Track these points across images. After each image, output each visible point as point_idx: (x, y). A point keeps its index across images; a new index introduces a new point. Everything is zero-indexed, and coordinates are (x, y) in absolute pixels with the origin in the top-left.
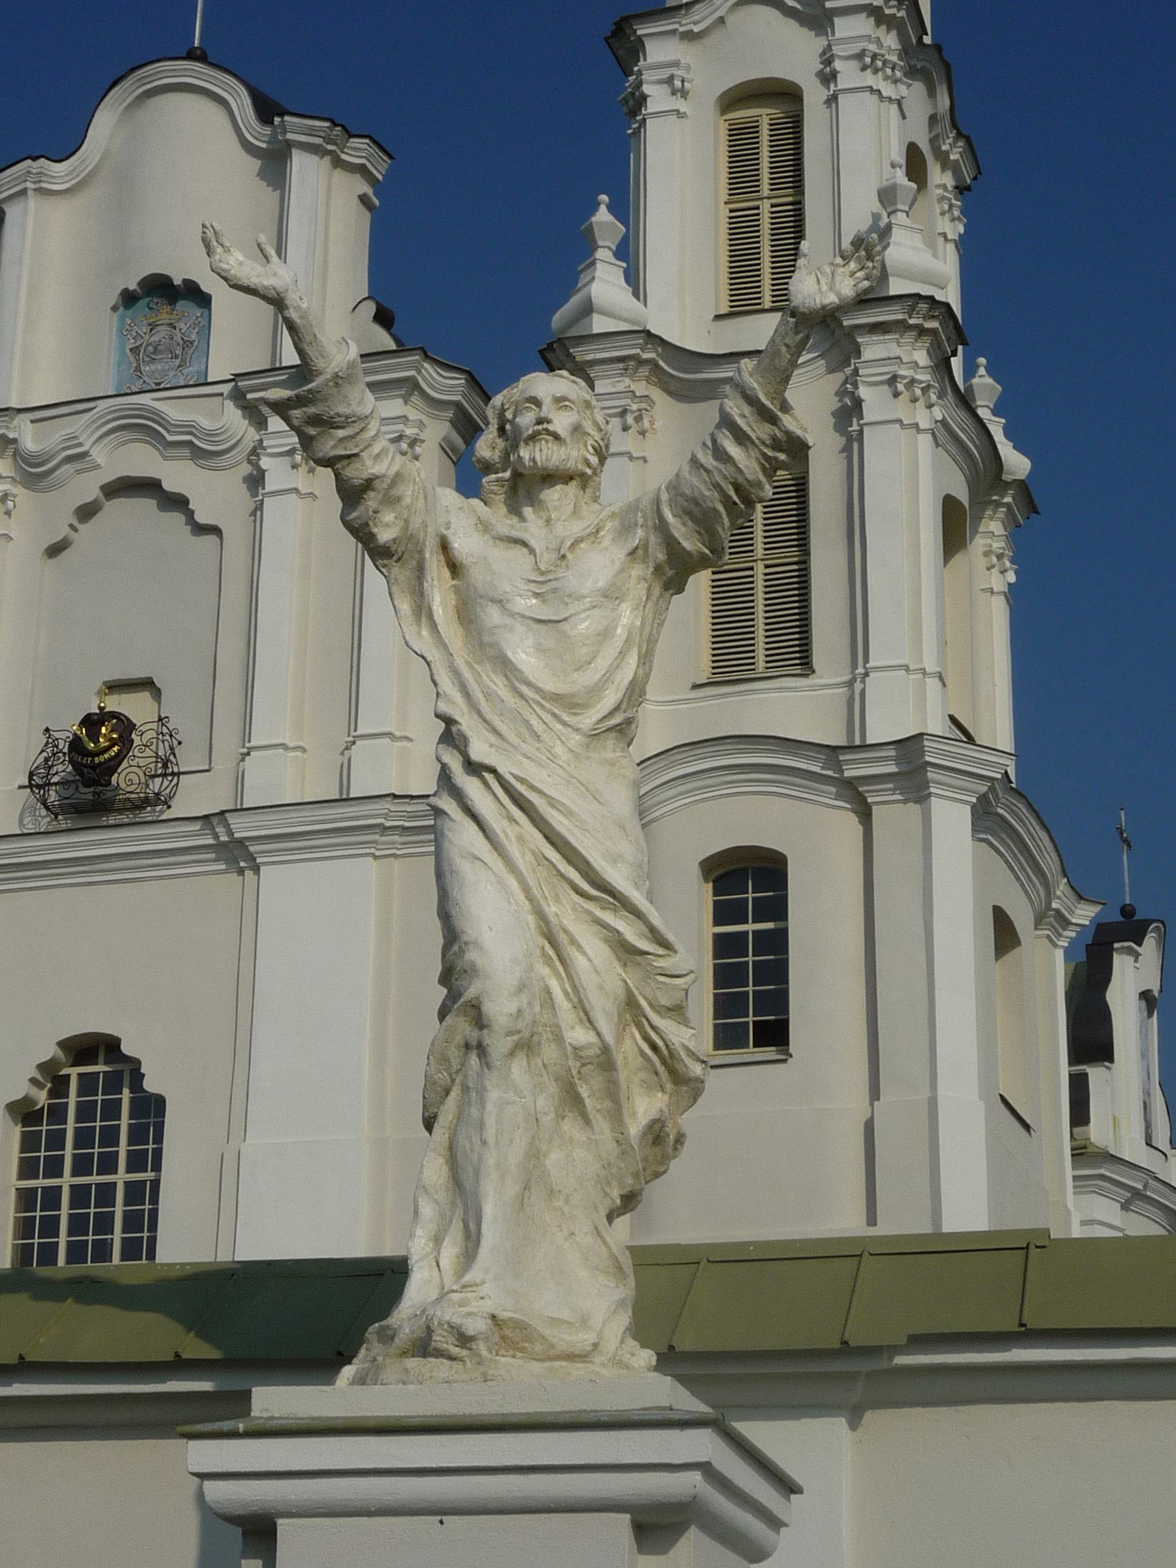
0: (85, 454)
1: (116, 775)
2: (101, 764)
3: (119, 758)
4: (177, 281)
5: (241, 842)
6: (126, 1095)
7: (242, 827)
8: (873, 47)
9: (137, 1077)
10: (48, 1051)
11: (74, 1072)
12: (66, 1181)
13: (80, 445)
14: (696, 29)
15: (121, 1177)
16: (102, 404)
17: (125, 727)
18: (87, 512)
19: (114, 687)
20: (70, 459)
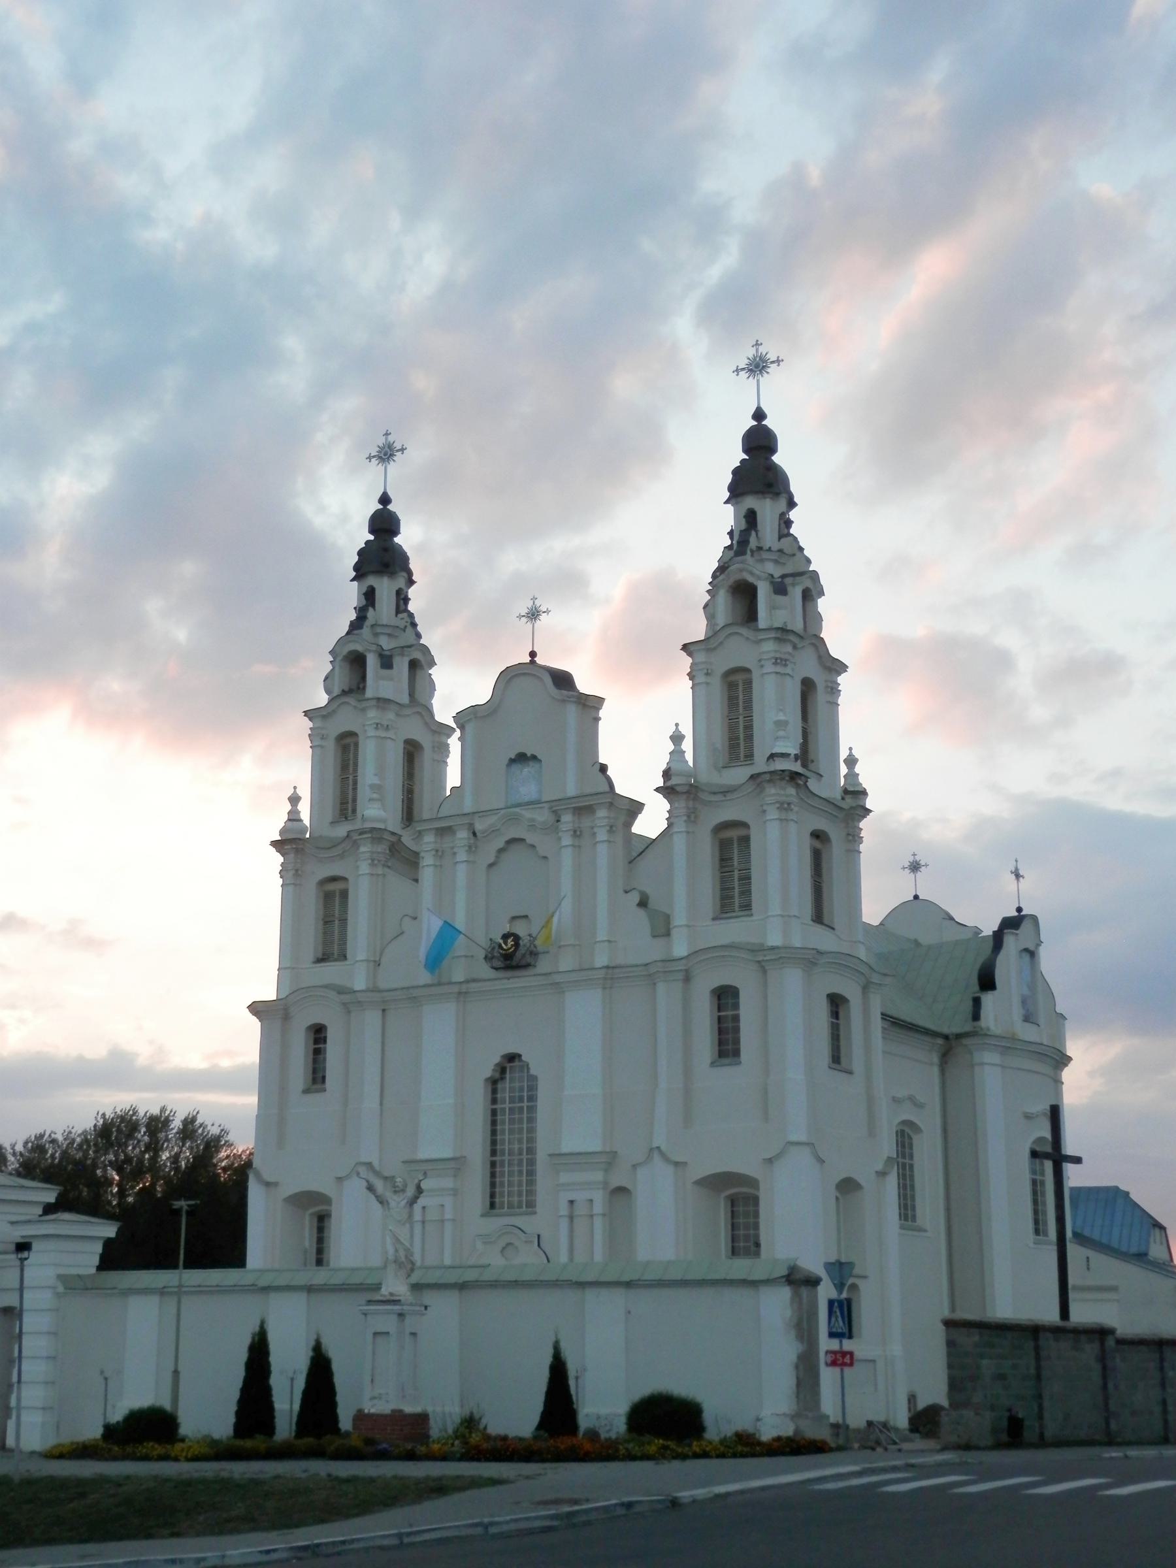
3: (515, 951)
4: (529, 755)
5: (557, 983)
6: (526, 1074)
7: (557, 978)
8: (778, 655)
9: (528, 1069)
10: (497, 1059)
11: (508, 1065)
12: (507, 1106)
14: (713, 646)
15: (525, 1104)
16: (502, 812)
17: (517, 938)
18: (501, 851)
19: (514, 918)
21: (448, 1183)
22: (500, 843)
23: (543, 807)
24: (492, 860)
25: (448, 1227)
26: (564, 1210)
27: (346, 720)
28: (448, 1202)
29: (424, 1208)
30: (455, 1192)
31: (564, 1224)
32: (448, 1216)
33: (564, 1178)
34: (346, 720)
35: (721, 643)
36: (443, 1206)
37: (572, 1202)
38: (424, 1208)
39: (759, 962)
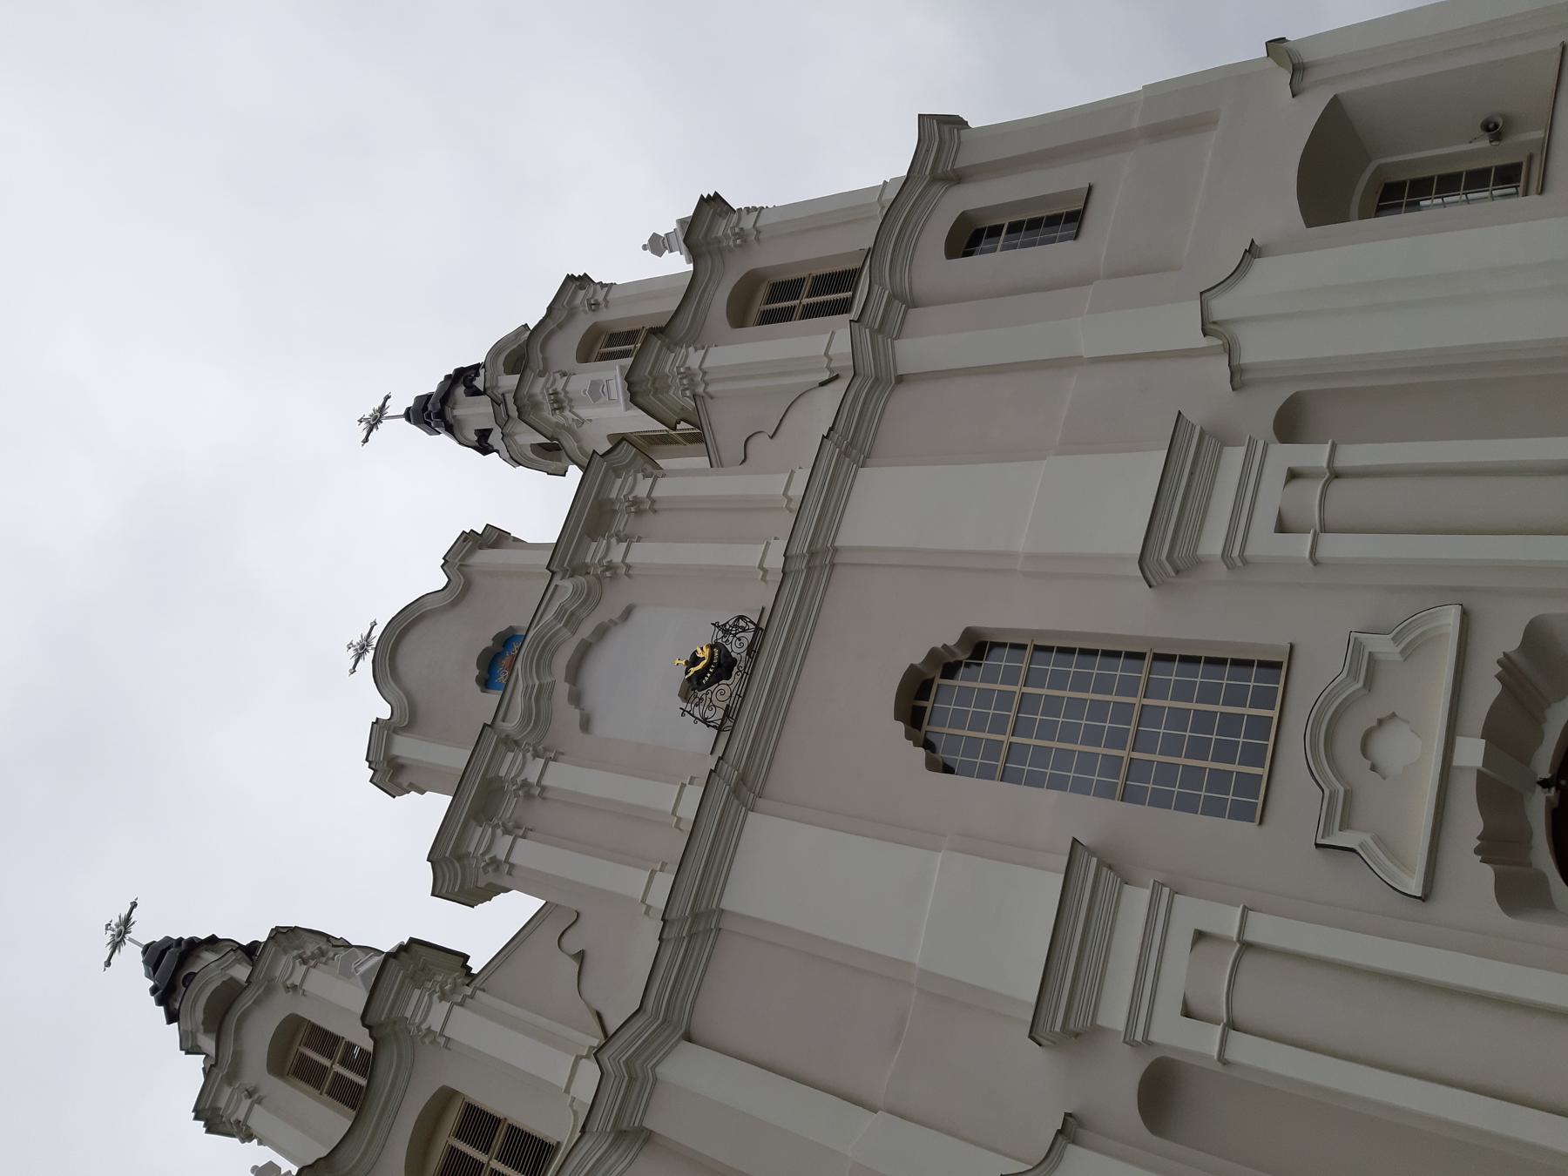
0: (541, 686)
1: (732, 654)
2: (719, 659)
13: (533, 686)
20: (537, 699)
21: (1136, 901)
22: (563, 689)
23: (556, 586)
24: (575, 714)
25: (1263, 930)
26: (1300, 545)
27: (259, 1033)
28: (1190, 914)
29: (1187, 1013)
30: (1167, 890)
31: (1335, 547)
32: (1226, 922)
33: (1212, 544)
34: (259, 1033)
35: (544, 359)
36: (1200, 936)
37: (1281, 527)
38: (1187, 1013)
39: (935, 179)
